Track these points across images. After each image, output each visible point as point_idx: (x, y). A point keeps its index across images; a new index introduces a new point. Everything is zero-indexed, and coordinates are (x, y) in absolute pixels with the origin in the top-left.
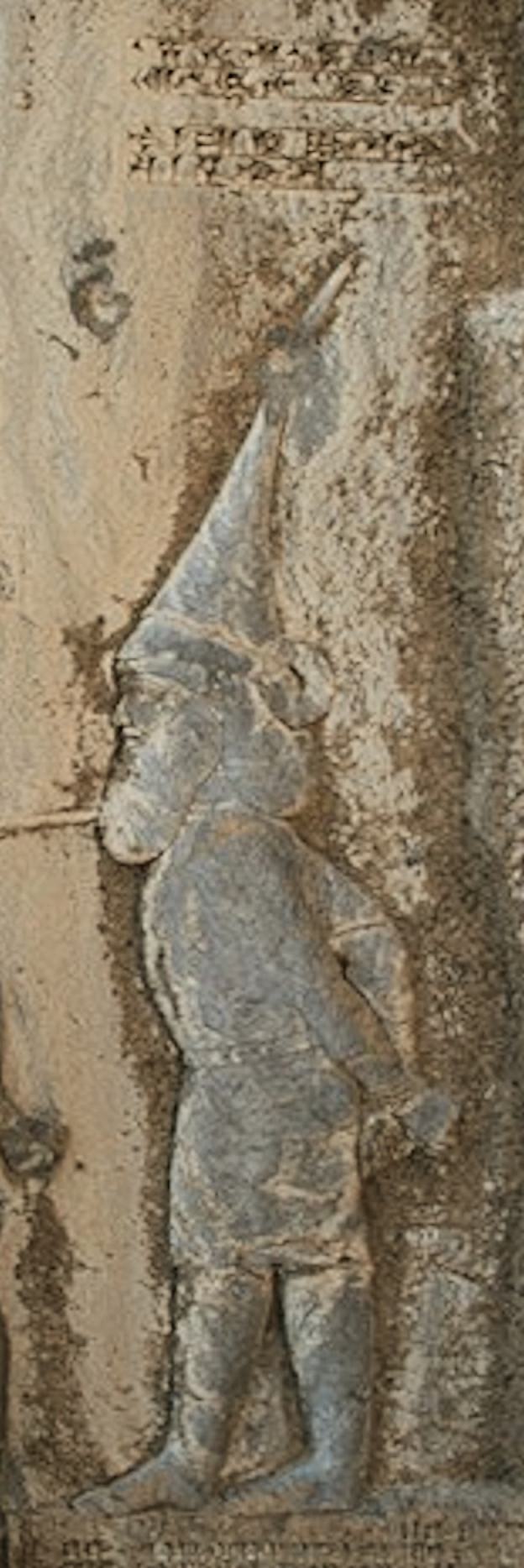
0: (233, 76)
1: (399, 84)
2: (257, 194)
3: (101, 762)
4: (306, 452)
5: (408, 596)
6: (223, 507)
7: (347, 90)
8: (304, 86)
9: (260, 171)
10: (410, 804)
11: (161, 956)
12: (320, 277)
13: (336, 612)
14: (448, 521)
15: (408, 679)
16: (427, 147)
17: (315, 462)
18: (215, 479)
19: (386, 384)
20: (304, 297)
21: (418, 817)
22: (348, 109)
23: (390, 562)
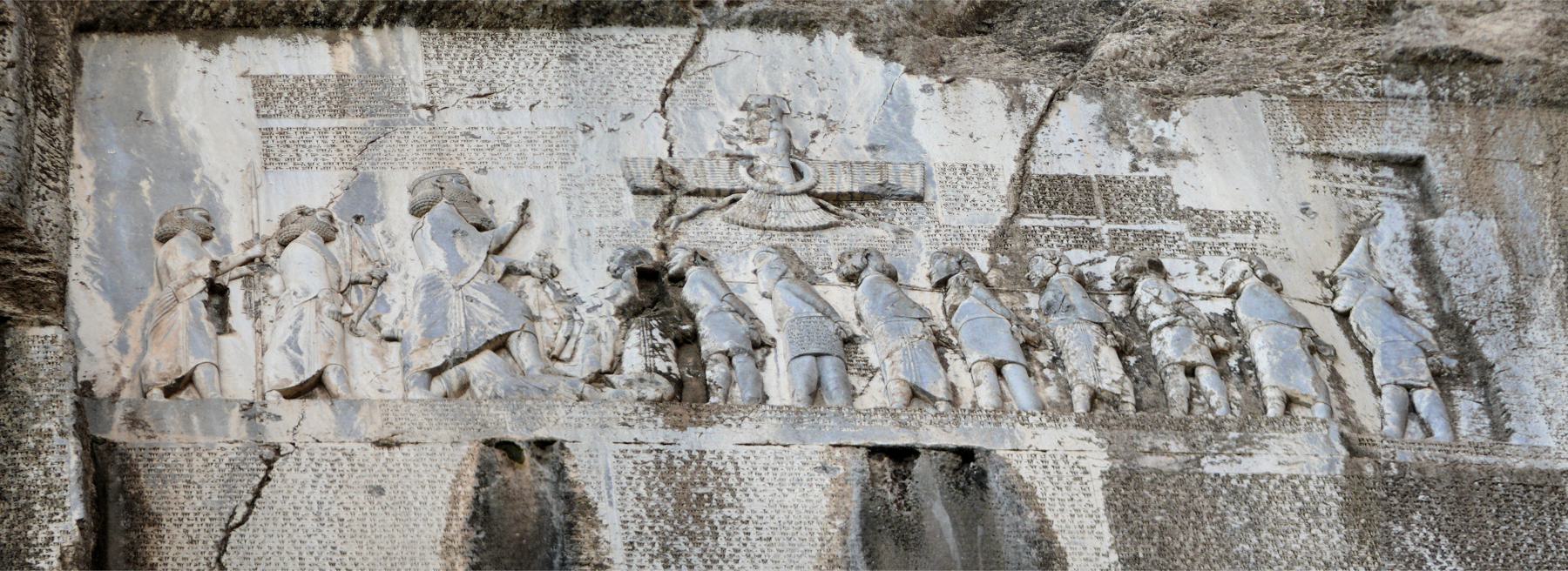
0: (1337, 180)
1: (1388, 184)
2: (1350, 200)
3: (1330, 296)
4: (1377, 244)
5: (1413, 271)
6: (1352, 256)
7: (1372, 184)
8: (1358, 182)
9: (1350, 196)
10: (1426, 307)
11: (1358, 325)
12: (1372, 216)
13: (1393, 272)
14: (1422, 260)
15: (1418, 285)
16: (1399, 197)
17: (1379, 247)
18: (1351, 249)
19: (1397, 234)
20: (1369, 220)
21: (1428, 310)
22: (1372, 188)
23: (1407, 265)
